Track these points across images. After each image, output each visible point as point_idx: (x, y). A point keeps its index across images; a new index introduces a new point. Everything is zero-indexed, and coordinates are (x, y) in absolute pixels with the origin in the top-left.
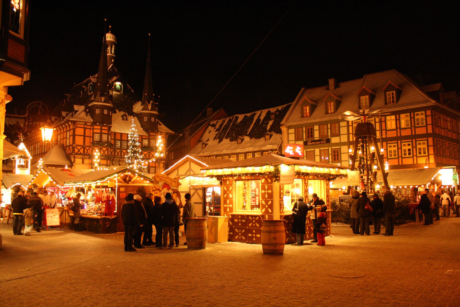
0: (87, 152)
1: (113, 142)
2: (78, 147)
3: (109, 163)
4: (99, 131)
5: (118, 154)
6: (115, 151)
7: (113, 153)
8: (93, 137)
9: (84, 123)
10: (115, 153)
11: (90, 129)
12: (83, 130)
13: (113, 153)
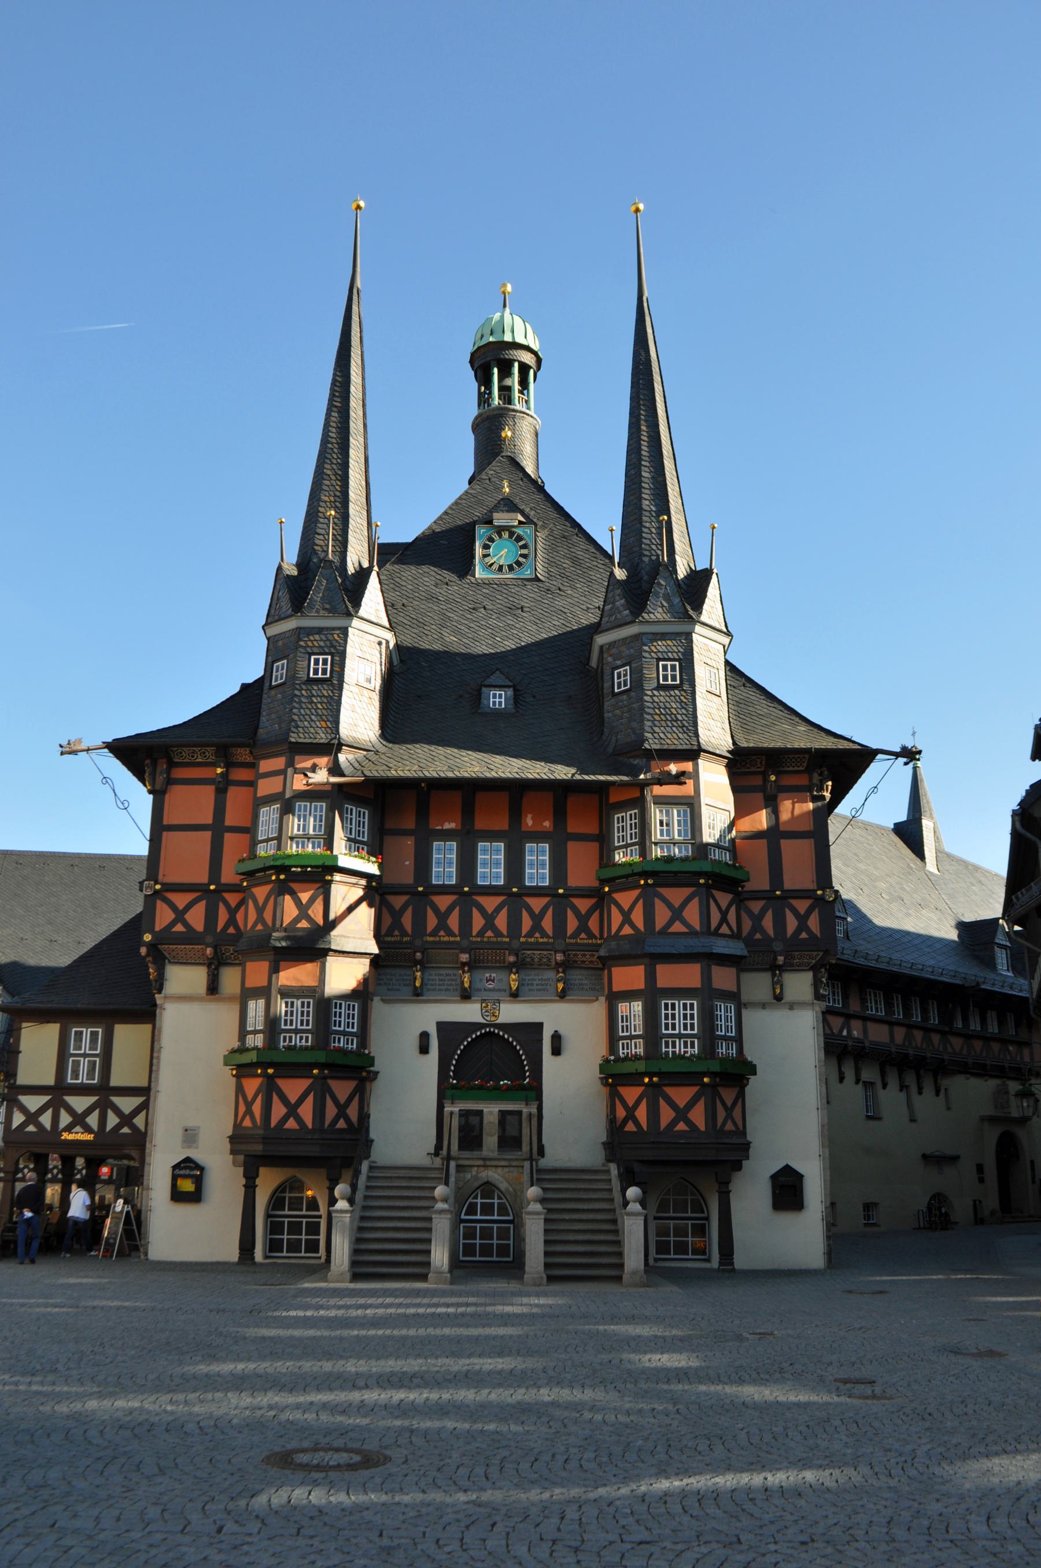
0: (232, 921)
2: (173, 897)
5: (442, 925)
10: (419, 921)
12: (208, 793)
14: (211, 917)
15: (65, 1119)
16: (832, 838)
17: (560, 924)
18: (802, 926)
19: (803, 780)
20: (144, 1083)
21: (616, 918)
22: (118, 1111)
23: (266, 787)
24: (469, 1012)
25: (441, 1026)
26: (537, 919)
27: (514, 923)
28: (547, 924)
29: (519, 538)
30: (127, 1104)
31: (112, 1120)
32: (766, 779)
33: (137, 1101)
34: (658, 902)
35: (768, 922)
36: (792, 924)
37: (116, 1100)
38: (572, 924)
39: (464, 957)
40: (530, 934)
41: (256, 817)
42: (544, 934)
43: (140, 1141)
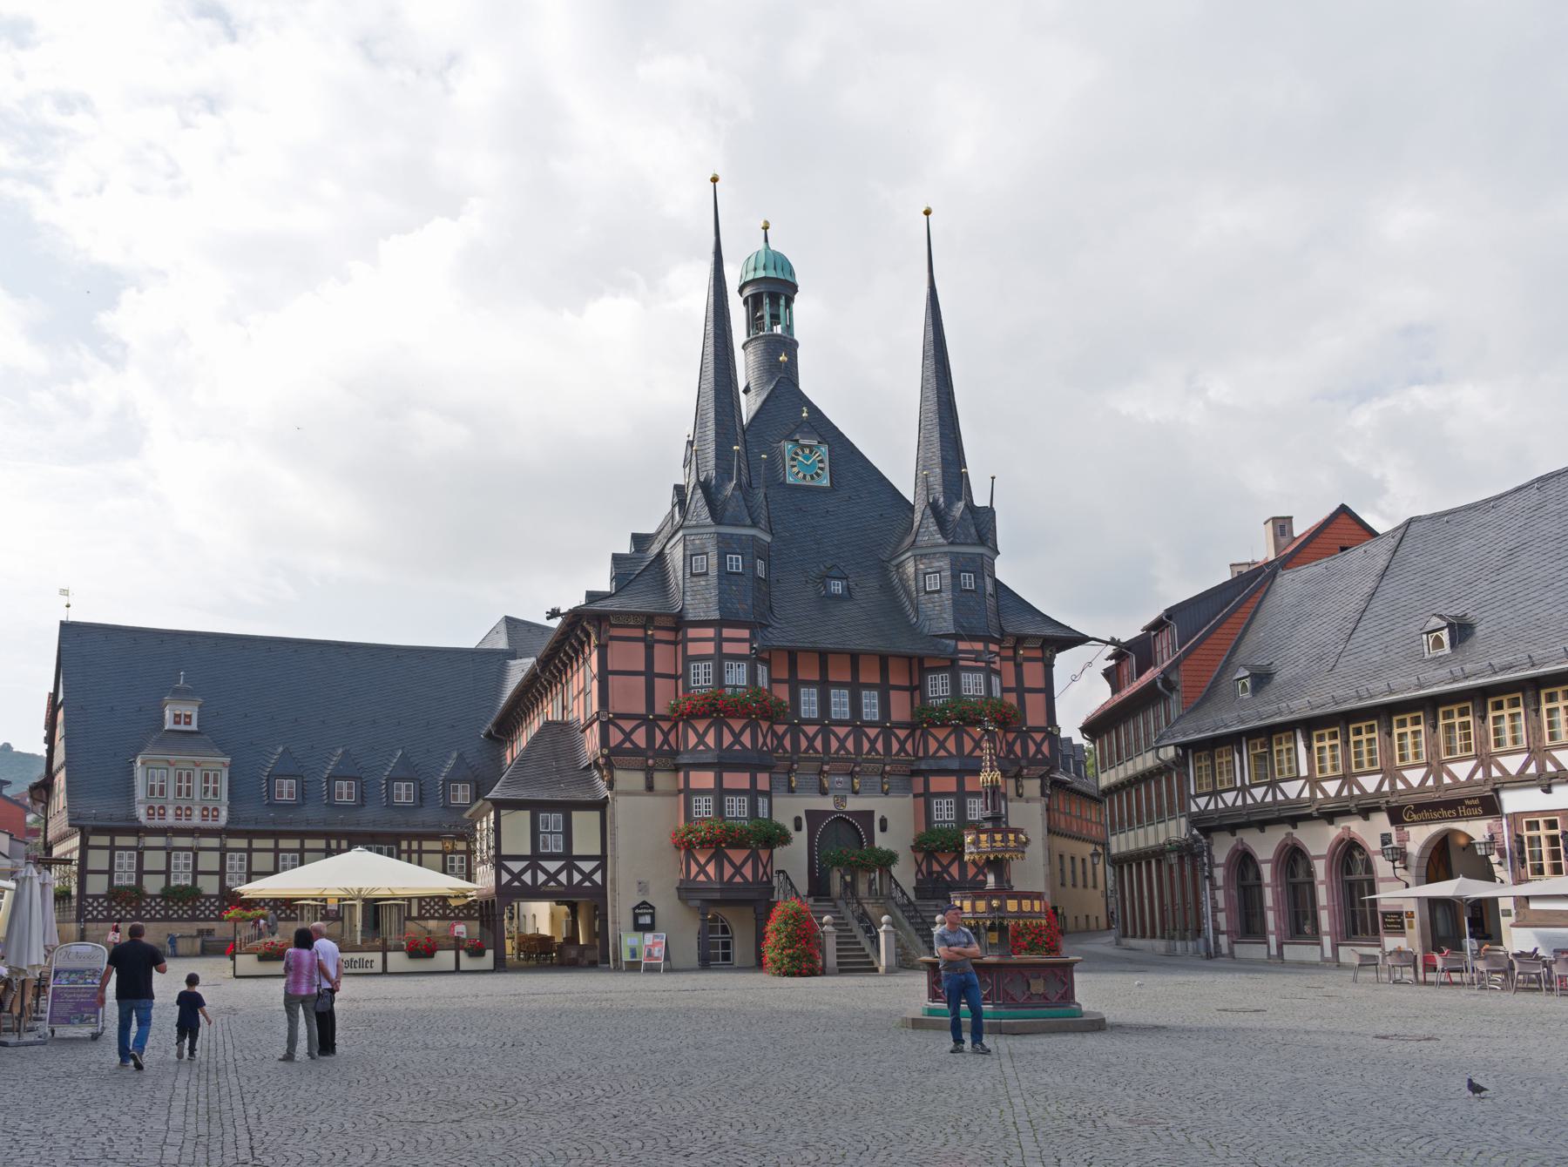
1: (782, 693)
5: (811, 746)
6: (796, 729)
7: (787, 742)
8: (686, 675)
9: (641, 621)
10: (795, 742)
13: (787, 742)
14: (650, 737)
15: (541, 878)
16: (1056, 693)
17: (887, 746)
18: (1039, 750)
19: (1038, 654)
20: (598, 852)
22: (580, 871)
24: (826, 804)
25: (809, 813)
26: (873, 742)
27: (858, 745)
28: (879, 746)
30: (587, 866)
31: (577, 877)
32: (1015, 652)
33: (595, 863)
35: (1018, 748)
36: (1032, 749)
37: (579, 864)
38: (895, 747)
39: (826, 768)
40: (869, 753)
41: (686, 670)
42: (878, 753)
43: (599, 893)
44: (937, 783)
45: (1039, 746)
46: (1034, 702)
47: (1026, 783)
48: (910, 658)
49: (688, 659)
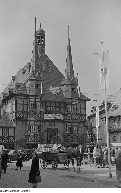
3: (41, 124)
4: (34, 100)
11: (28, 99)
14: (23, 116)
18: (83, 119)
21: (67, 117)
22: (10, 140)
23: (31, 100)
29: (49, 66)
30: (11, 138)
31: (10, 141)
33: (13, 138)
34: (73, 116)
44: (68, 124)
45: (83, 118)
46: (83, 110)
47: (81, 124)
48: (64, 102)
49: (30, 102)
